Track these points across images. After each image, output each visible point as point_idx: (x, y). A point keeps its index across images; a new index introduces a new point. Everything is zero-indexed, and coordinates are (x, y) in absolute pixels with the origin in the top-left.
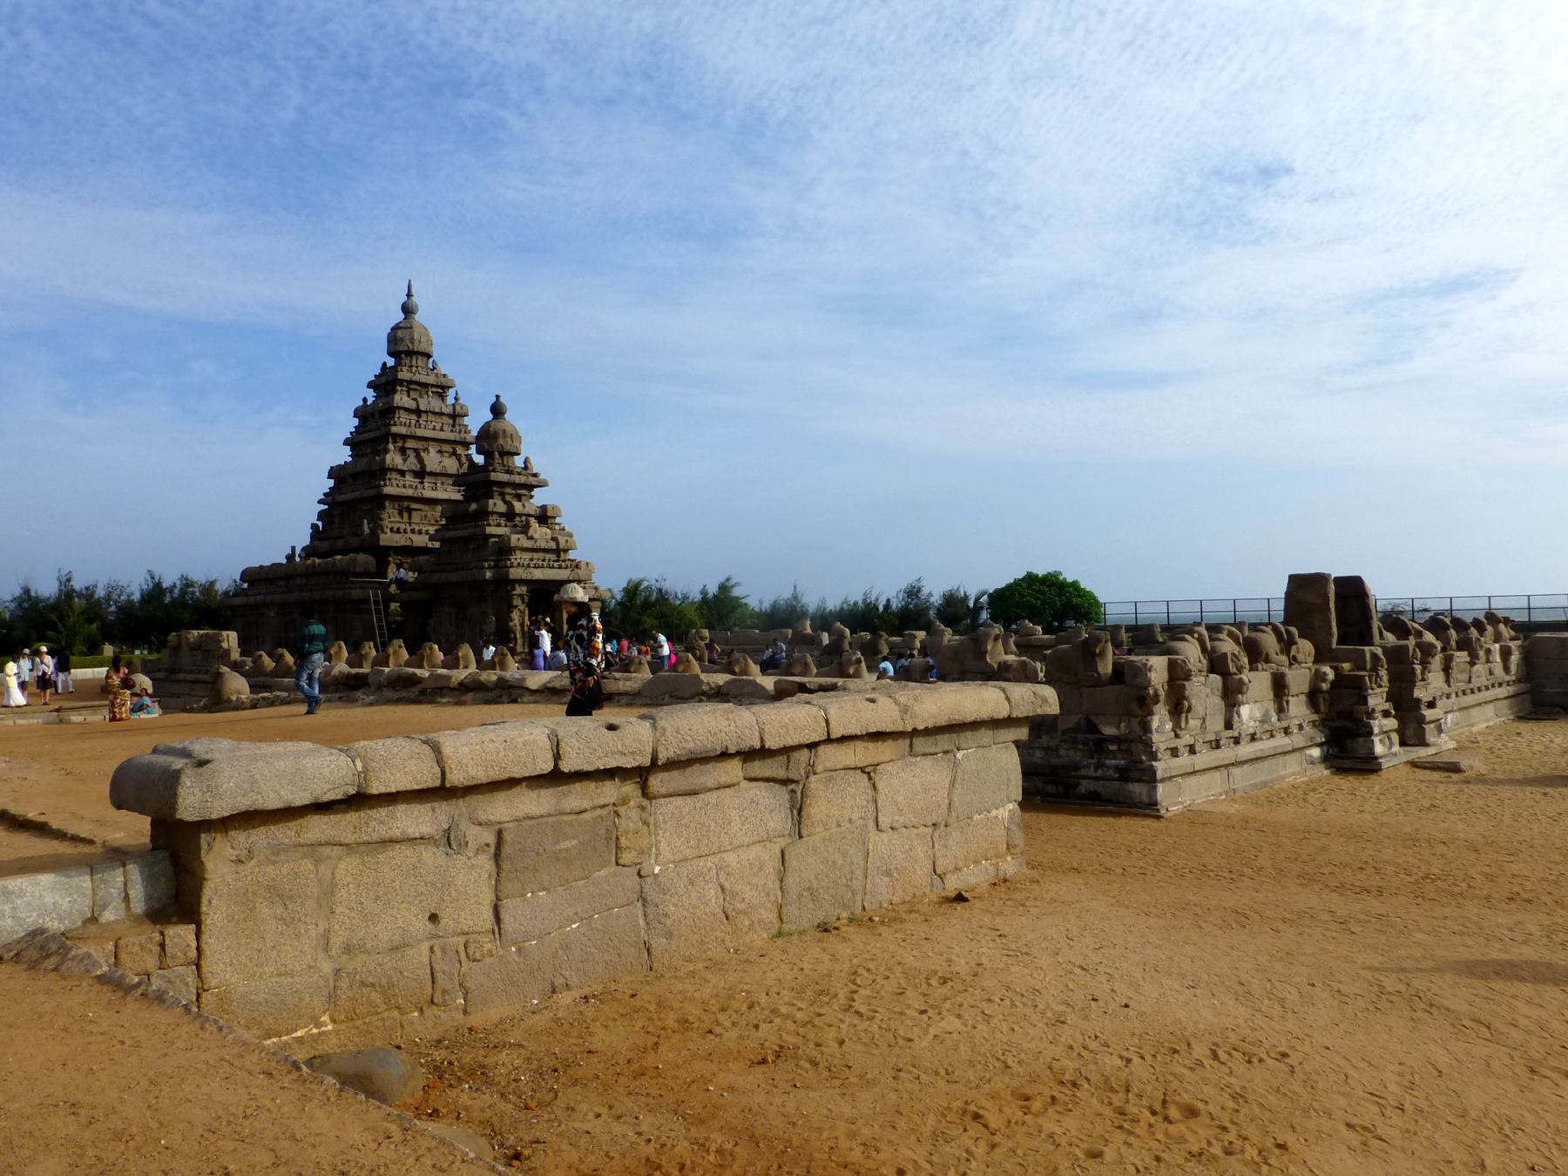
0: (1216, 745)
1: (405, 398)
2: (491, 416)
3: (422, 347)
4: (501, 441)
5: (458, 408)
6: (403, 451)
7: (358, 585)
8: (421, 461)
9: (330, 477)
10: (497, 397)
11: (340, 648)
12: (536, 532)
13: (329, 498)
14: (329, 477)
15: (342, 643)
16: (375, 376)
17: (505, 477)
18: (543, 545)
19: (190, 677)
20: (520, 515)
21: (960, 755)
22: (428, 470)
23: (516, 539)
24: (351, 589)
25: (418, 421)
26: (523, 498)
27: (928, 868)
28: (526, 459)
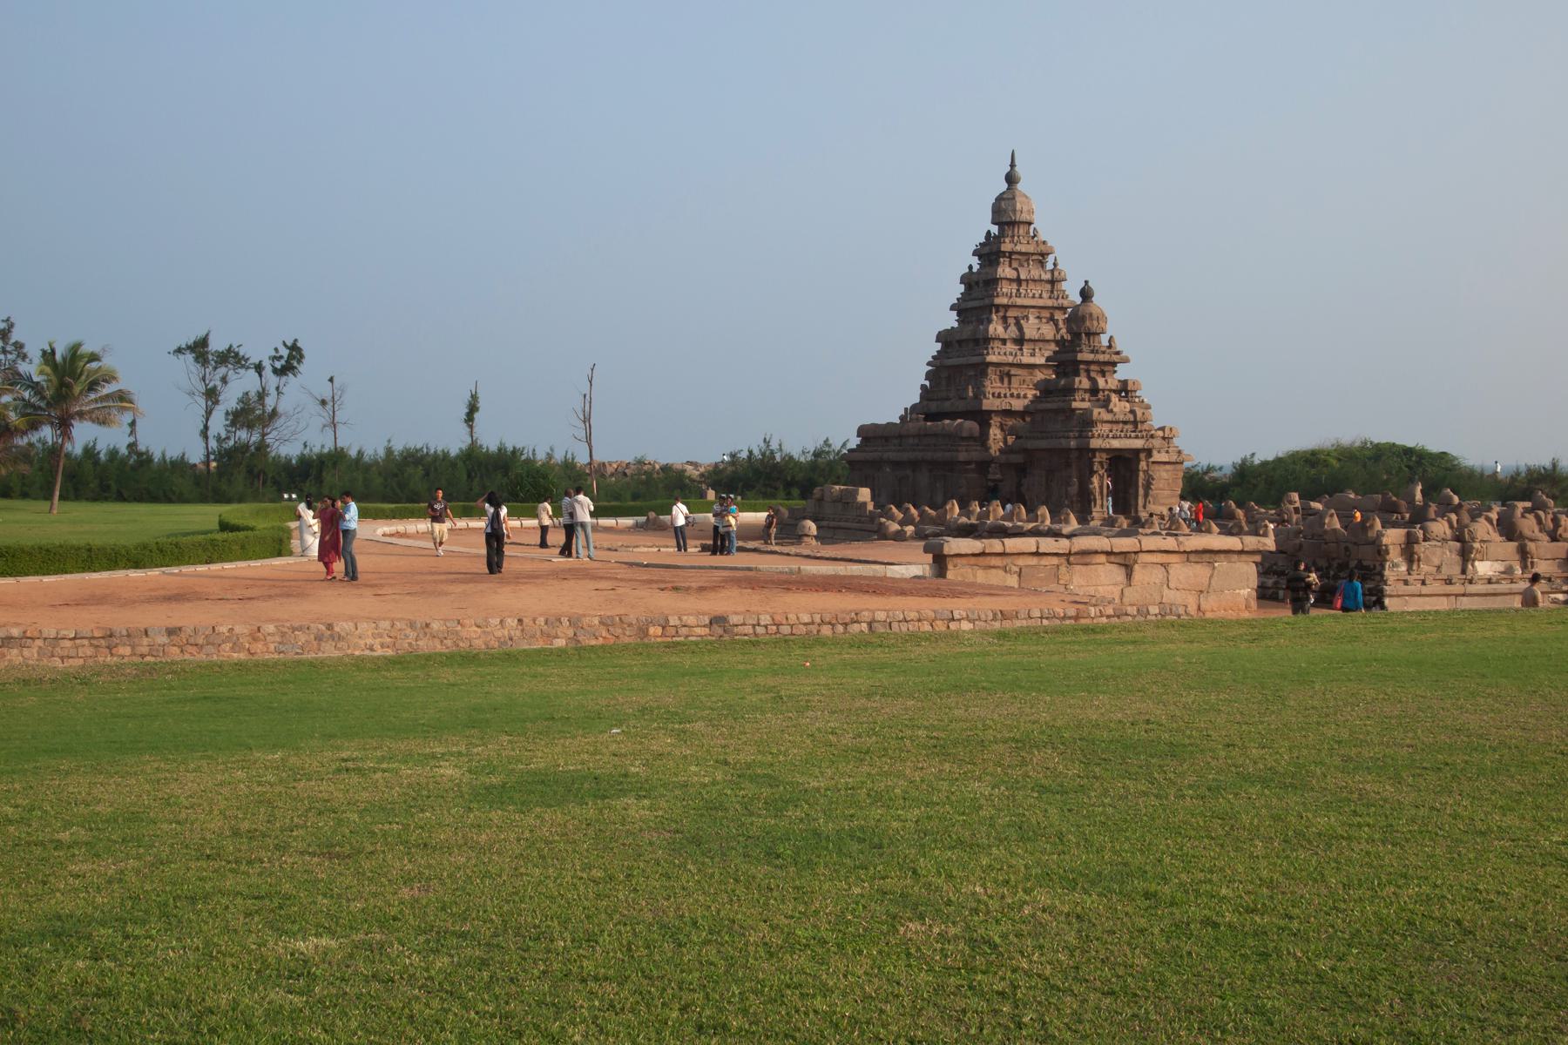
0: (1449, 582)
1: (1008, 270)
3: (1025, 217)
4: (1088, 323)
5: (1056, 274)
6: (1005, 319)
7: (964, 448)
8: (1020, 329)
9: (937, 341)
10: (1086, 282)
11: (953, 505)
12: (1115, 406)
14: (937, 341)
15: (955, 501)
17: (1090, 357)
18: (1121, 418)
19: (832, 524)
20: (1103, 391)
21: (1216, 564)
22: (1027, 337)
23: (1098, 413)
24: (957, 451)
25: (1018, 290)
27: (1195, 607)
28: (1111, 337)
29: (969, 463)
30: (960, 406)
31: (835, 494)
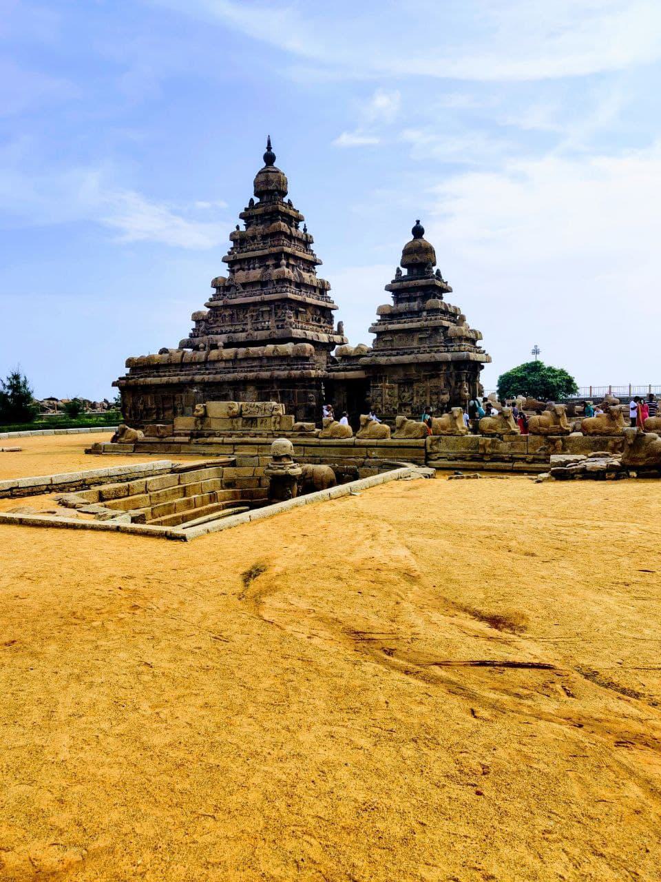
2: (413, 237)
5: (309, 236)
8: (300, 275)
29: (312, 379)
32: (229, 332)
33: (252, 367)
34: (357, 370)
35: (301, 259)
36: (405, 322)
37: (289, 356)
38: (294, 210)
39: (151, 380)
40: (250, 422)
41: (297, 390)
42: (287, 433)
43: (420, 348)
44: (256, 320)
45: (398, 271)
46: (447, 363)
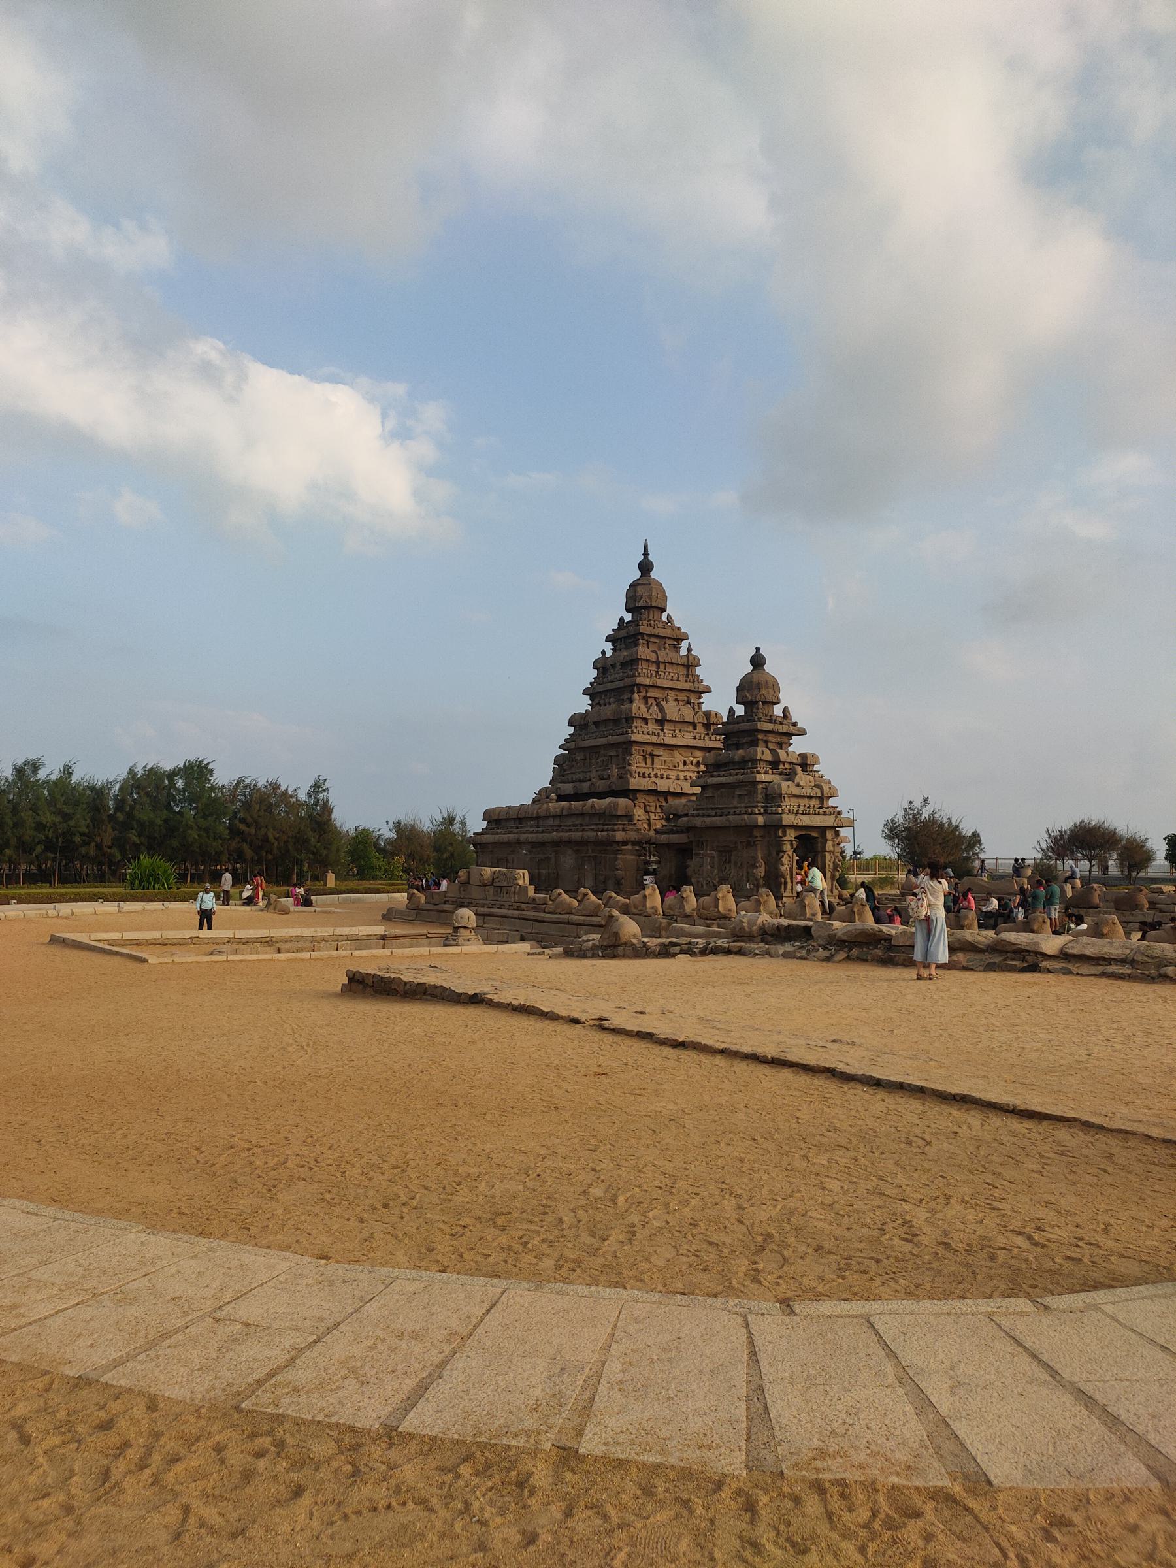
2: (751, 668)
4: (763, 691)
5: (691, 658)
8: (662, 709)
9: (570, 724)
10: (758, 649)
11: (654, 890)
13: (571, 745)
14: (570, 724)
16: (613, 630)
17: (769, 727)
18: (809, 792)
20: (784, 763)
23: (786, 787)
24: (614, 830)
25: (657, 672)
26: (784, 746)
29: (625, 843)
30: (601, 786)
31: (486, 877)
32: (580, 781)
33: (574, 825)
34: (682, 832)
35: (671, 689)
36: (724, 776)
37: (604, 813)
38: (673, 628)
39: (488, 838)
40: (499, 890)
41: (608, 856)
42: (523, 906)
43: (737, 808)
44: (607, 766)
45: (731, 710)
46: (757, 826)
